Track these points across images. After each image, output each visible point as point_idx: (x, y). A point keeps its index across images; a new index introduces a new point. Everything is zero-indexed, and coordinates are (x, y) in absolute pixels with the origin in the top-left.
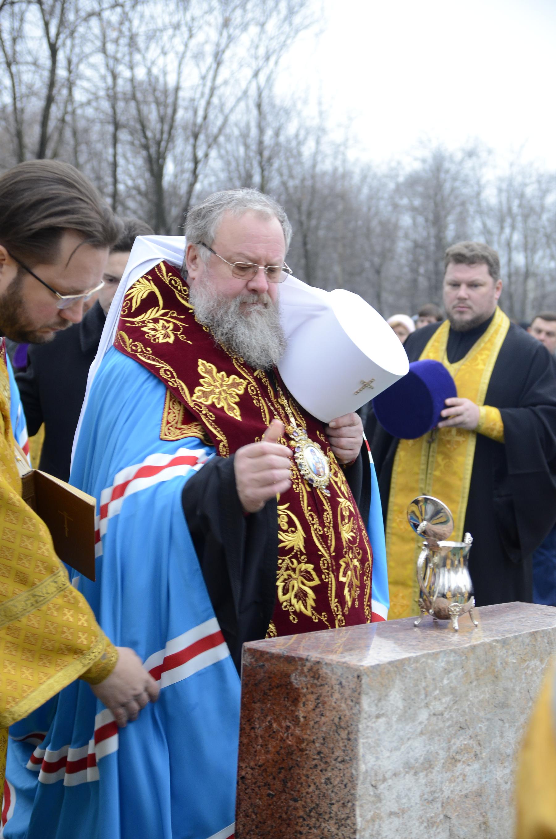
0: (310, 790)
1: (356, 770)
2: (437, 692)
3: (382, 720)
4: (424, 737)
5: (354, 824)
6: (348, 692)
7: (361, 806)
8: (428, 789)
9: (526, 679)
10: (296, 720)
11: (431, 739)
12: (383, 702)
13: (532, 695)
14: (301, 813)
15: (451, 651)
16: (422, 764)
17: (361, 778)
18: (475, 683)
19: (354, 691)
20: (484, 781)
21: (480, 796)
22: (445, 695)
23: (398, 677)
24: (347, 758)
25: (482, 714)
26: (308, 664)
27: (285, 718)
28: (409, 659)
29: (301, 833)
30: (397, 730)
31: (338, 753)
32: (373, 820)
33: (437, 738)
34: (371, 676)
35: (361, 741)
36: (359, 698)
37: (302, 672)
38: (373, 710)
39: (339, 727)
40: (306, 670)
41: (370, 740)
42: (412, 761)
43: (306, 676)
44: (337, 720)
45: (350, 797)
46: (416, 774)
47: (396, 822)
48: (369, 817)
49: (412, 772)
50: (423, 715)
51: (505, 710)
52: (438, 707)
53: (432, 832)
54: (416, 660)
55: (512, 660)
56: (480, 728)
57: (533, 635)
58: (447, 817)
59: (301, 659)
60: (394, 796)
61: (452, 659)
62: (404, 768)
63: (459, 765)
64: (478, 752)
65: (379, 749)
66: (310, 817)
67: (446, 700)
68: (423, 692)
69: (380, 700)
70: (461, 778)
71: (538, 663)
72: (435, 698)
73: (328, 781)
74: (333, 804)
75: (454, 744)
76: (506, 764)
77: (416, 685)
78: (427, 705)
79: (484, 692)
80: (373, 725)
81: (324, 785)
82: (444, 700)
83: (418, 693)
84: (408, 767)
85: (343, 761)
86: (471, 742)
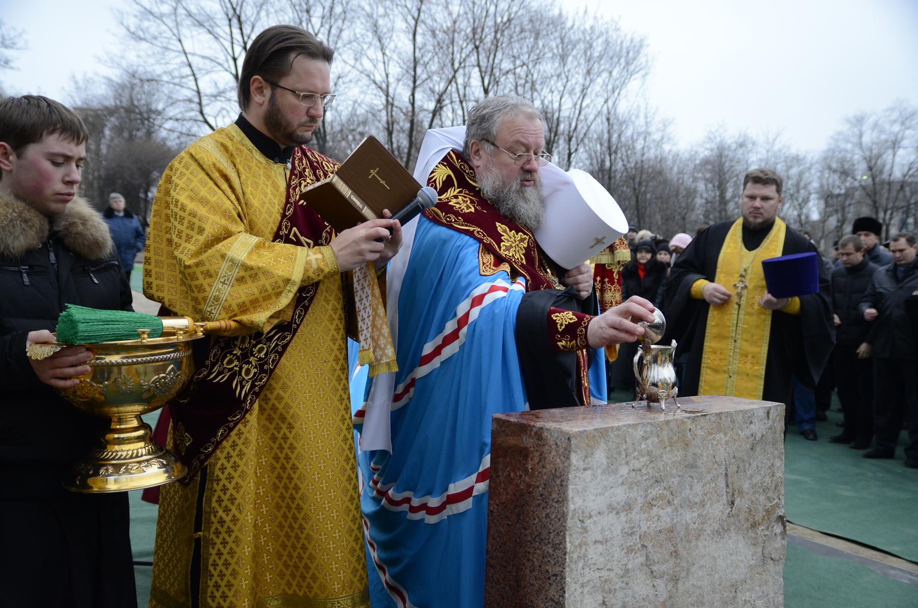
0: (536, 522)
1: (567, 508)
2: (636, 453)
3: (588, 472)
5: (565, 548)
6: (561, 450)
7: (570, 535)
8: (628, 525)
9: (712, 447)
10: (526, 470)
11: (631, 488)
12: (589, 459)
13: (717, 460)
14: (529, 539)
15: (648, 423)
16: (623, 506)
17: (570, 514)
18: (668, 449)
19: (566, 449)
20: (675, 521)
21: (672, 532)
22: (643, 456)
23: (602, 440)
24: (560, 499)
25: (674, 471)
26: (535, 429)
27: (519, 469)
28: (612, 428)
29: (529, 553)
31: (554, 495)
32: (580, 546)
33: (635, 488)
34: (579, 438)
35: (570, 487)
36: (569, 455)
37: (530, 435)
38: (581, 465)
39: (555, 476)
40: (533, 434)
41: (578, 487)
42: (615, 505)
43: (533, 439)
44: (553, 471)
45: (562, 528)
46: (617, 513)
47: (601, 548)
48: (577, 543)
49: (614, 512)
50: (624, 470)
51: (694, 469)
52: (638, 465)
53: (631, 556)
54: (618, 428)
55: (700, 433)
56: (673, 482)
57: (719, 415)
58: (643, 546)
59: (530, 426)
60: (599, 529)
61: (648, 429)
62: (608, 509)
63: (655, 508)
64: (671, 500)
66: (536, 542)
67: (645, 459)
68: (624, 453)
69: (586, 457)
70: (656, 518)
71: (723, 436)
72: (634, 458)
73: (547, 515)
74: (550, 533)
75: (651, 493)
76: (695, 509)
77: (618, 447)
78: (627, 463)
79: (676, 455)
81: (544, 519)
82: (641, 460)
83: (619, 453)
84: (611, 508)
85: (558, 502)
86: (665, 492)
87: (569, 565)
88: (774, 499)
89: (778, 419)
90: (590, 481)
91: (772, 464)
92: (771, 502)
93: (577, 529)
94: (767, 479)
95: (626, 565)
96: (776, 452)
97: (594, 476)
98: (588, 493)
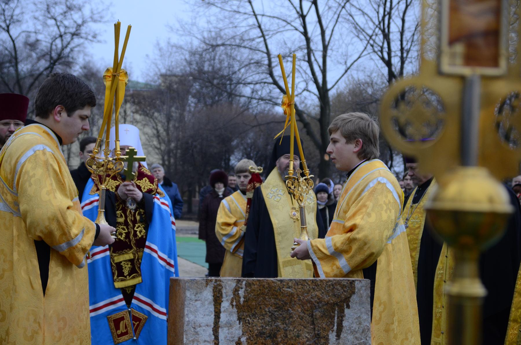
4: (226, 313)
7: (187, 335)
8: (230, 335)
12: (199, 295)
16: (225, 324)
17: (186, 323)
30: (208, 307)
35: (186, 309)
48: (191, 339)
65: (196, 313)
69: (197, 294)
80: (194, 303)
88: (362, 339)
89: (363, 288)
90: (200, 307)
91: (359, 317)
92: (358, 340)
93: (191, 332)
94: (354, 326)
96: (363, 310)
97: (203, 304)
98: (199, 313)
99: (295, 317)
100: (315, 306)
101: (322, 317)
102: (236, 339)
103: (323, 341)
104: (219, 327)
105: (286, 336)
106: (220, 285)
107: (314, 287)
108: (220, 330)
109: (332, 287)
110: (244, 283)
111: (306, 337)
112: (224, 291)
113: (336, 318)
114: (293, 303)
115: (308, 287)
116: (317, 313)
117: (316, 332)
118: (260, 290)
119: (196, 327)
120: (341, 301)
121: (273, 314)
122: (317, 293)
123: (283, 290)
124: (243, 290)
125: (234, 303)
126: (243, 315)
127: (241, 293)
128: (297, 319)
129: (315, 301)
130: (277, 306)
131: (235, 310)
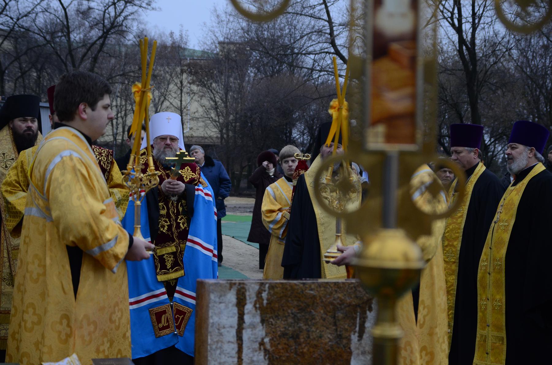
7: (211, 336)
8: (253, 336)
12: (223, 298)
17: (210, 325)
32: (217, 342)
48: (215, 340)
69: (221, 296)
87: (210, 351)
95: (251, 358)
97: (227, 307)
99: (318, 319)
100: (338, 308)
101: (344, 318)
102: (260, 340)
103: (345, 341)
104: (243, 329)
105: (309, 337)
106: (244, 288)
107: (336, 289)
108: (244, 331)
109: (354, 289)
110: (267, 286)
111: (329, 338)
112: (247, 294)
113: (358, 319)
114: (316, 304)
115: (330, 289)
116: (340, 315)
117: (339, 333)
118: (283, 292)
119: (221, 329)
120: (363, 303)
121: (295, 316)
122: (340, 295)
123: (306, 293)
124: (266, 292)
125: (258, 306)
126: (266, 317)
127: (264, 295)
128: (320, 320)
129: (338, 303)
130: (300, 307)
131: (259, 312)
